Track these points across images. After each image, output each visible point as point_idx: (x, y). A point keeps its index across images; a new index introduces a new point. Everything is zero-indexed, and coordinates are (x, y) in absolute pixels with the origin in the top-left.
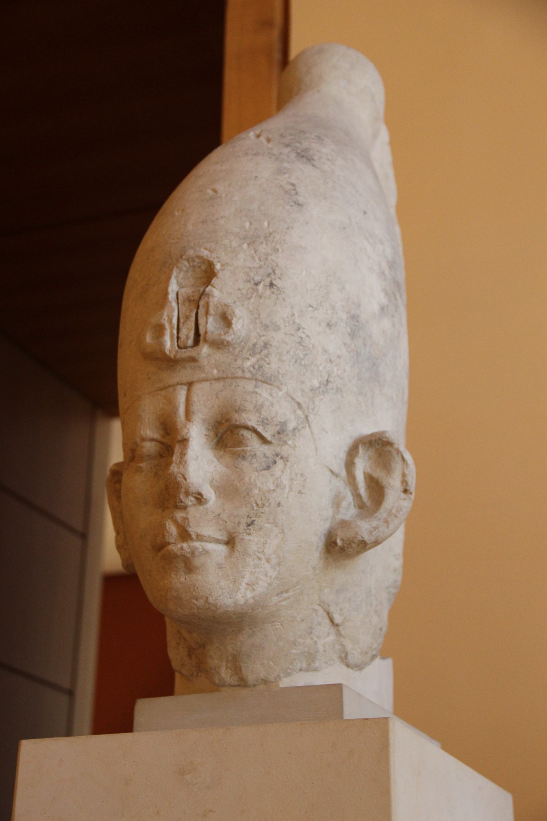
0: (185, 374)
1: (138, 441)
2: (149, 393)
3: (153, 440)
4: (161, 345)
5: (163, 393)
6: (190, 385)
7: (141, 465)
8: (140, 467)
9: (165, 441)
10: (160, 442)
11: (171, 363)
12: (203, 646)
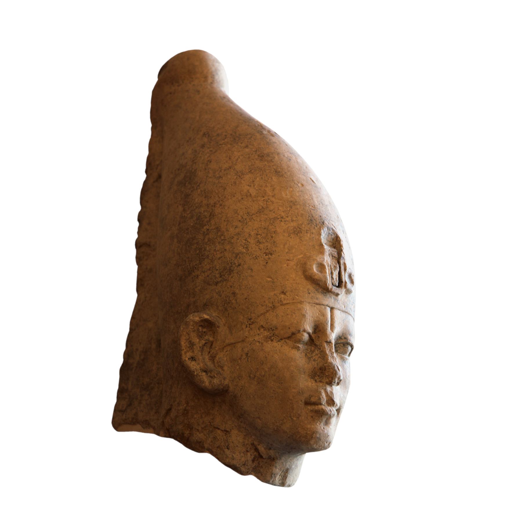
0: (330, 301)
1: (302, 330)
2: (309, 303)
3: (309, 333)
4: (326, 278)
5: (318, 306)
6: (332, 309)
7: (300, 346)
8: (299, 347)
9: (313, 336)
10: (310, 336)
11: (326, 290)
12: (274, 459)
